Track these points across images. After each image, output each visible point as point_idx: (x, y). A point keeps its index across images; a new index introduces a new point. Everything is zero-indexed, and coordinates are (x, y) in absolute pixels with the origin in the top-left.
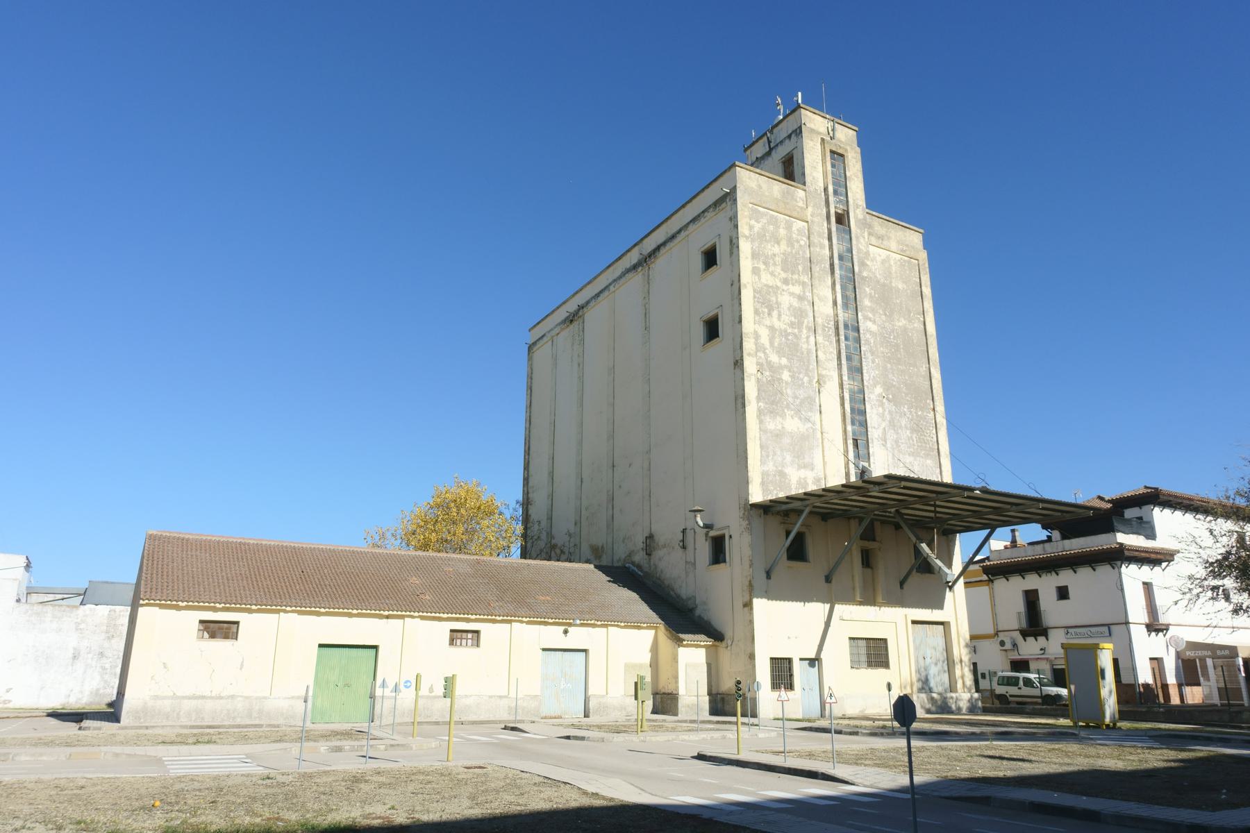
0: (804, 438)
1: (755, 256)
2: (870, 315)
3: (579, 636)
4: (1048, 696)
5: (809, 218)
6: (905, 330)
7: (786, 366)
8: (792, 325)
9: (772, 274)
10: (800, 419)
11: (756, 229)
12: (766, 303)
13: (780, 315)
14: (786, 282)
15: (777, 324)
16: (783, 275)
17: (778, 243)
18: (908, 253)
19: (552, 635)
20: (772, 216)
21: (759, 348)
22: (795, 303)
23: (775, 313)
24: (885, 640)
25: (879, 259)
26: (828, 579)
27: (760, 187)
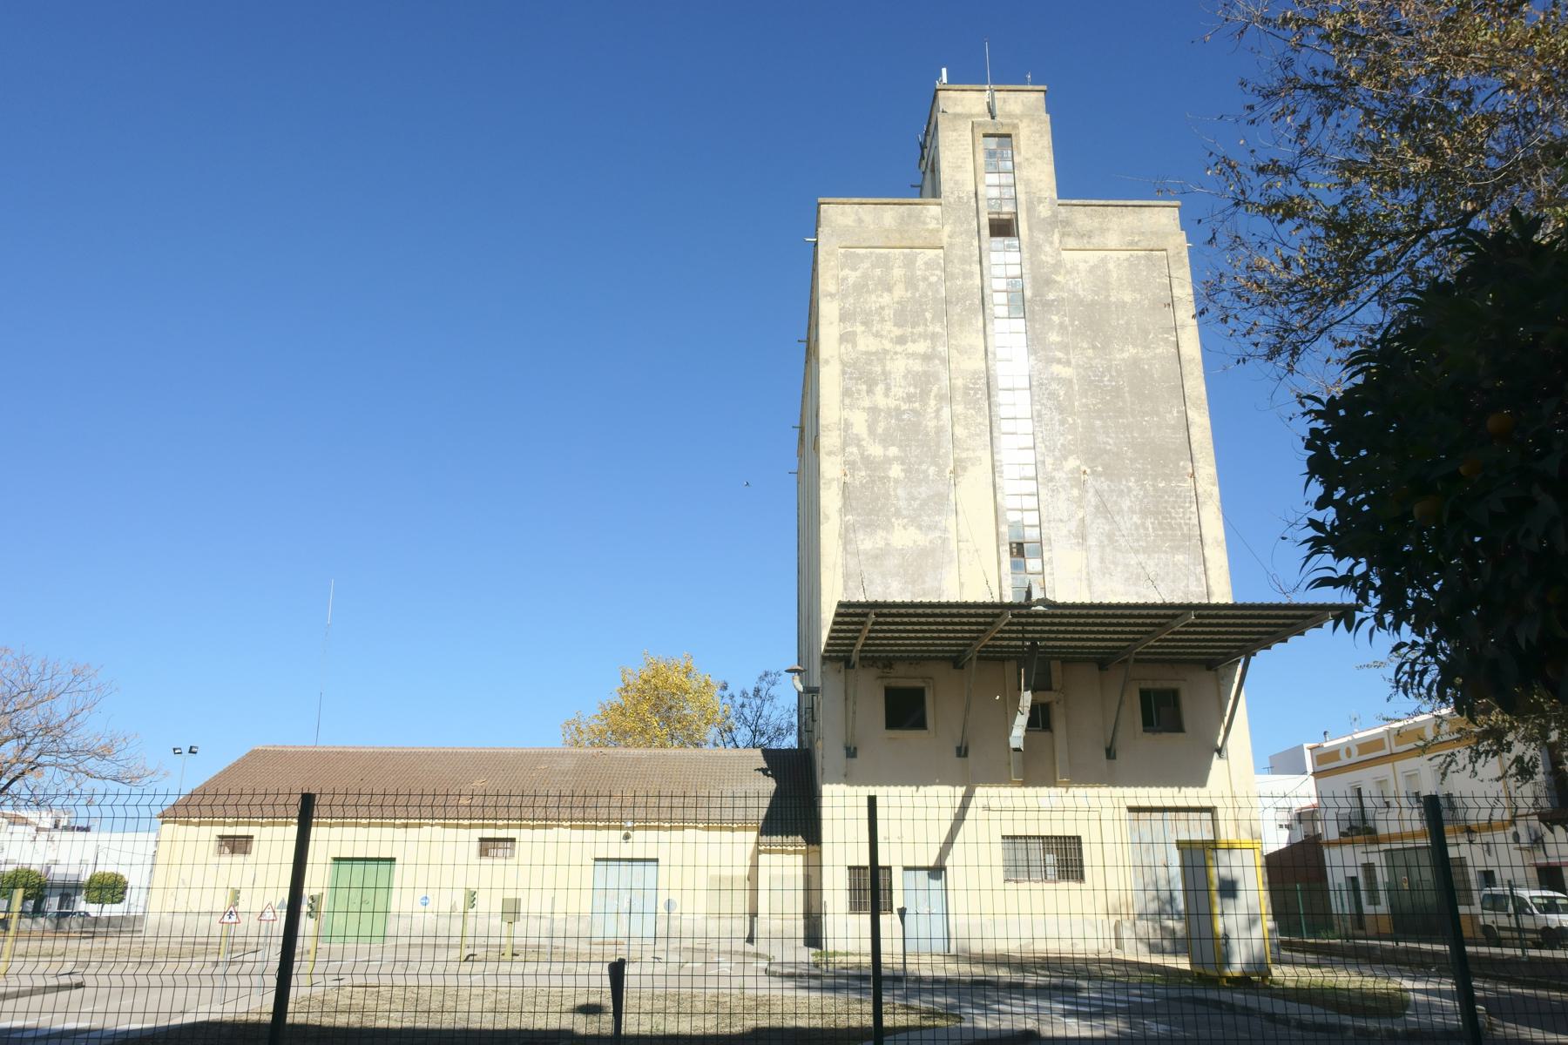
0: (924, 553)
1: (844, 317)
2: (1059, 354)
3: (643, 842)
4: (1547, 929)
5: (945, 241)
6: (1135, 362)
7: (896, 458)
8: (909, 398)
9: (877, 335)
10: (920, 527)
11: (851, 281)
12: (862, 375)
13: (888, 389)
14: (901, 340)
15: (881, 401)
16: (897, 332)
17: (890, 290)
18: (1144, 245)
19: (609, 842)
20: (879, 256)
21: (848, 439)
22: (917, 366)
23: (880, 389)
24: (1077, 840)
25: (1083, 267)
26: (1110, 753)
27: (860, 221)
